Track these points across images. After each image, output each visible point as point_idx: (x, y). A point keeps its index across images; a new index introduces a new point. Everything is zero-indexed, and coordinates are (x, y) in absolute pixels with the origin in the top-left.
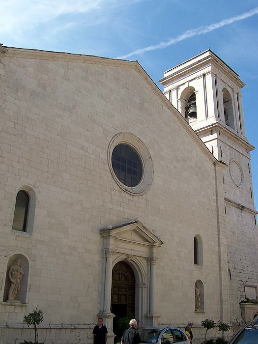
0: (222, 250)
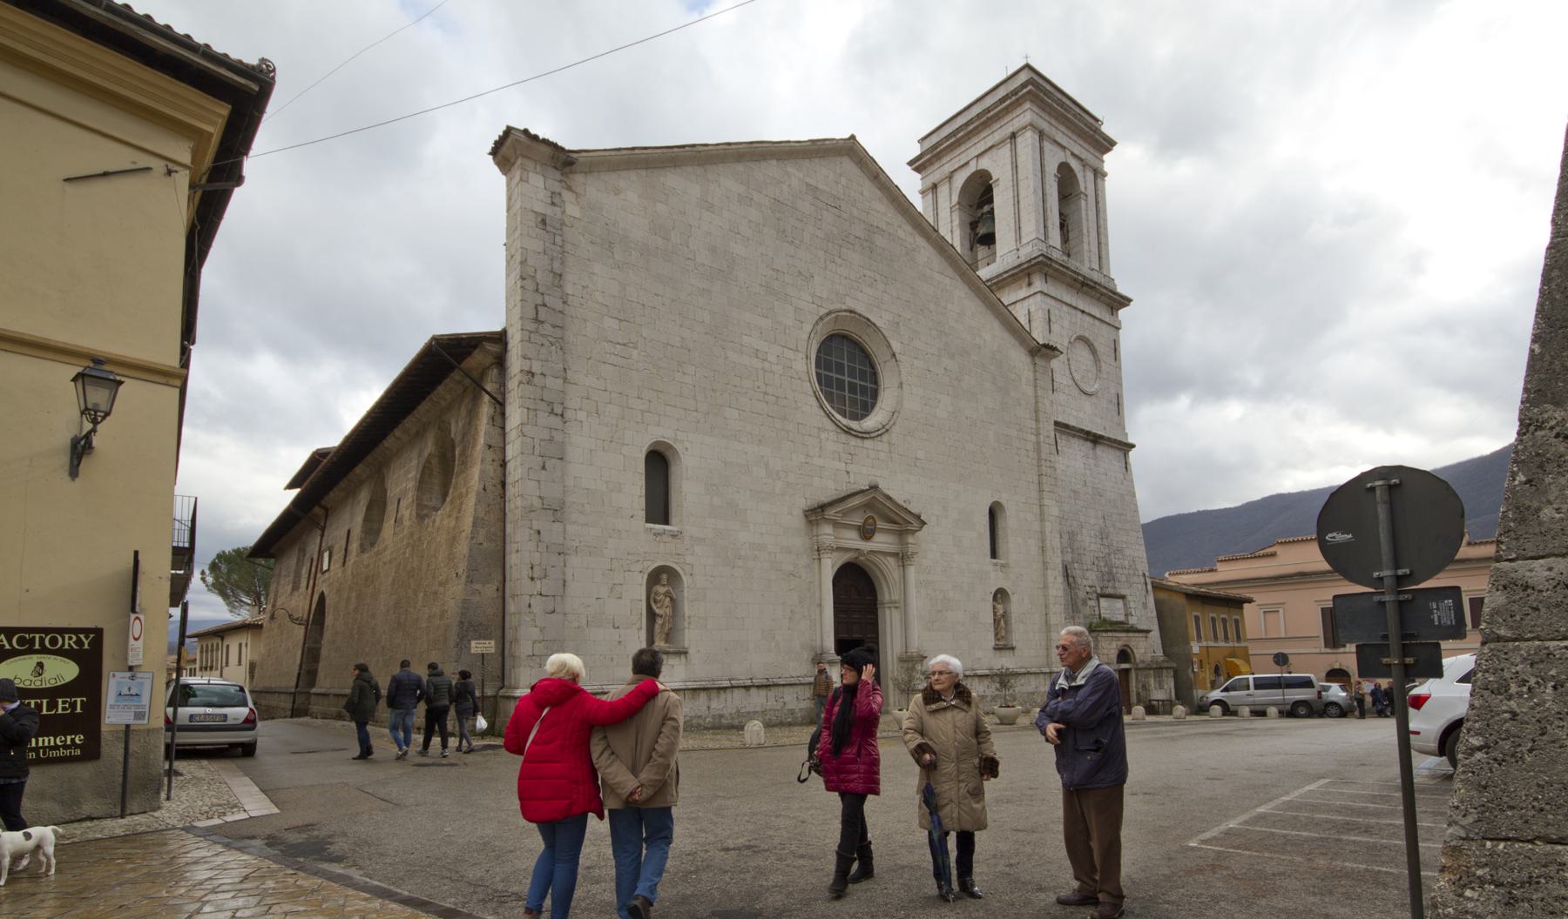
0: (1048, 530)
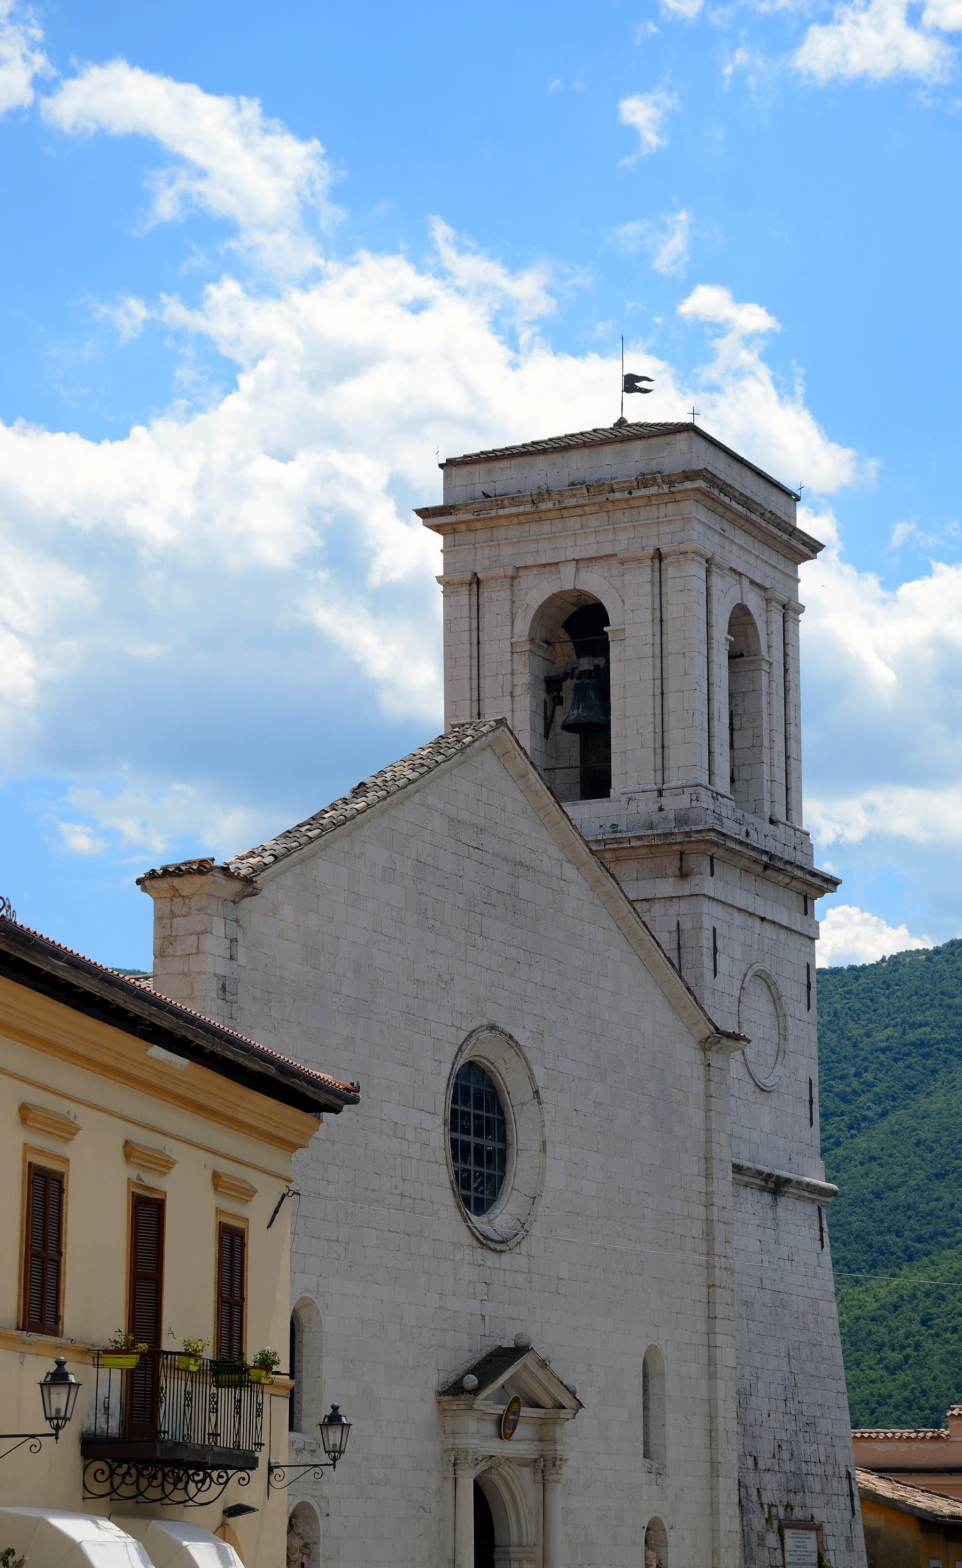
0: (721, 1395)
